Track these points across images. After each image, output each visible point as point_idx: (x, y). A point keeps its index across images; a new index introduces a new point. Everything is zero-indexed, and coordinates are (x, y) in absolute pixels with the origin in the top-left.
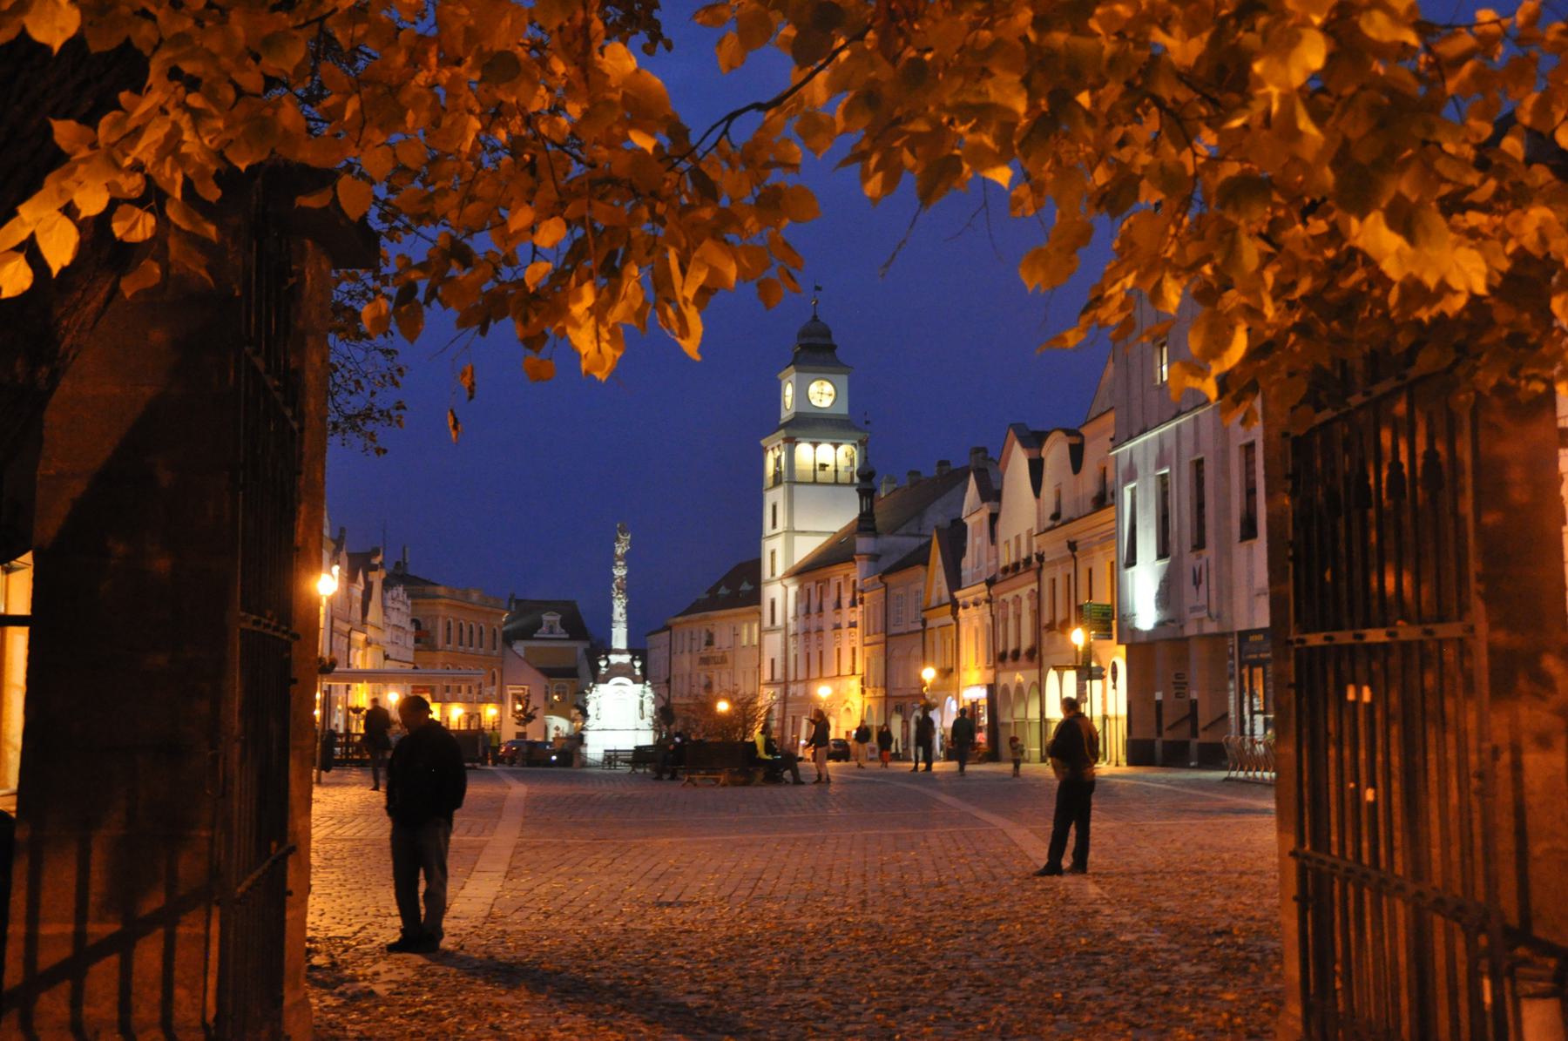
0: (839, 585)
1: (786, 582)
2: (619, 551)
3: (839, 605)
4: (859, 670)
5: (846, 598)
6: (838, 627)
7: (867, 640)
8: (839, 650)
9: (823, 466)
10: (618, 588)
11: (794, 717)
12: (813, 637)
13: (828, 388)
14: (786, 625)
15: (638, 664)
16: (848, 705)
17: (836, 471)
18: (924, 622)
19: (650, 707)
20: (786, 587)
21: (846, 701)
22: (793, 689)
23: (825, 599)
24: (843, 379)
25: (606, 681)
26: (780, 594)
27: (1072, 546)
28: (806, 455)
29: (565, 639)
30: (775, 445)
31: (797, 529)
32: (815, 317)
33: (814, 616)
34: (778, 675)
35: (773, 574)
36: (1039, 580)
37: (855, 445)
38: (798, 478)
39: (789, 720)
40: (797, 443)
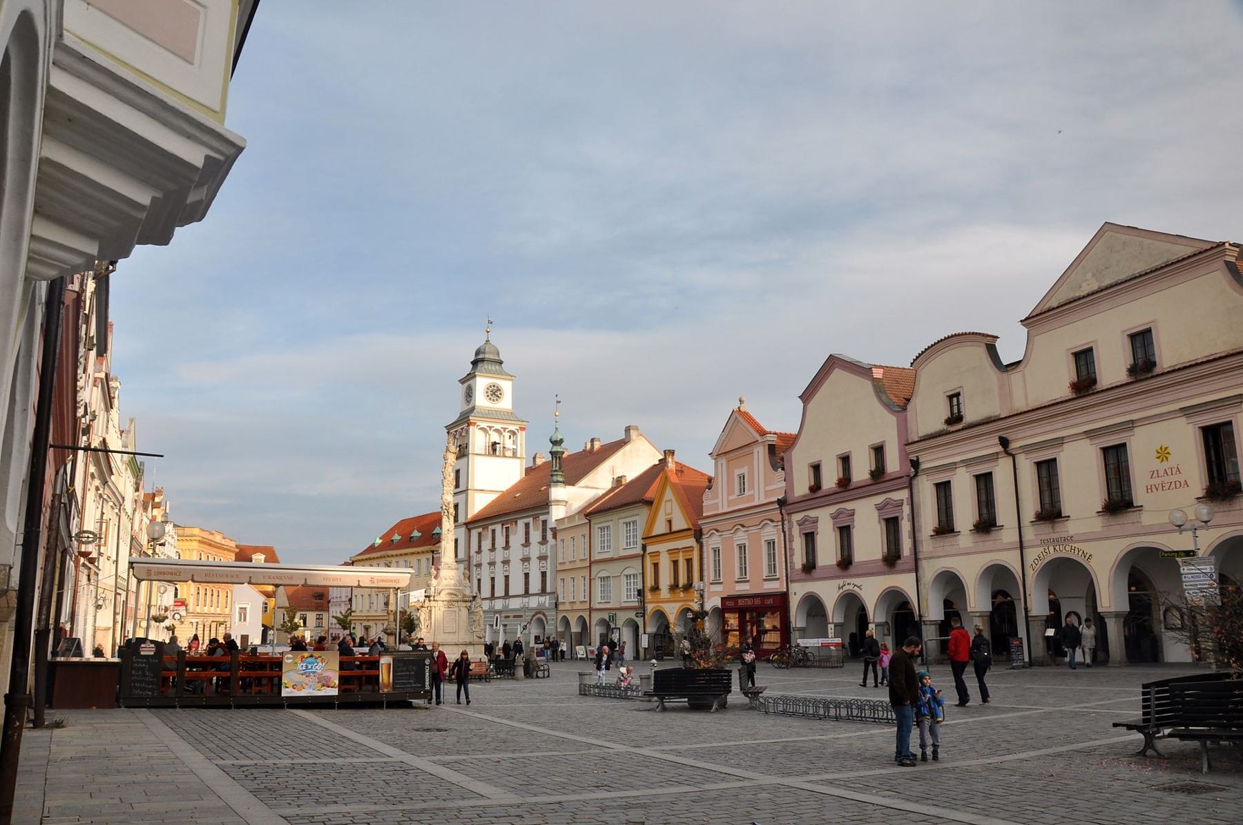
0: (527, 525)
1: (470, 526)
5: (536, 536)
12: (499, 565)
20: (469, 530)
23: (511, 538)
27: (1004, 442)
31: (476, 488)
36: (910, 487)
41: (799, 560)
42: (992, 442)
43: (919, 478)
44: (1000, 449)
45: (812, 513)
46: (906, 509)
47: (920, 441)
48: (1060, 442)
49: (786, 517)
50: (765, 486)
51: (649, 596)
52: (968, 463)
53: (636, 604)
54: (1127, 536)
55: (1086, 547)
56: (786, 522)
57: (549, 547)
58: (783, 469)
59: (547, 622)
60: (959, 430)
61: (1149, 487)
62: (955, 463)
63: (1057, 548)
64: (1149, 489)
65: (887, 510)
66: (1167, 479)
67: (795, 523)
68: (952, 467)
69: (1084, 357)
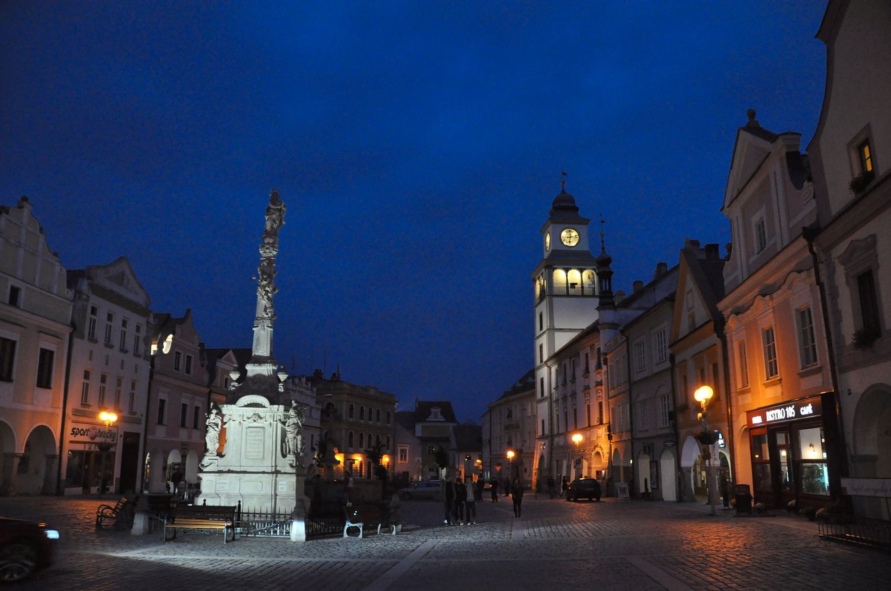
0: (587, 355)
1: (549, 363)
2: (268, 225)
3: (587, 371)
4: (604, 422)
5: (593, 363)
6: (587, 388)
7: (611, 394)
8: (589, 406)
9: (573, 285)
10: (263, 273)
11: (557, 461)
12: (569, 399)
13: (574, 233)
14: (551, 394)
15: (283, 377)
16: (598, 449)
17: (582, 287)
18: (672, 358)
19: (294, 441)
20: (550, 368)
21: (596, 446)
22: (556, 439)
24: (584, 228)
25: (232, 400)
26: (547, 374)
28: (560, 275)
29: (444, 421)
30: (540, 274)
31: (556, 328)
32: (563, 191)
33: (569, 384)
34: (547, 432)
35: (541, 361)
37: (595, 270)
38: (555, 292)
39: (555, 463)
40: (554, 269)
41: (849, 327)
45: (862, 234)
49: (822, 257)
50: (789, 219)
51: (680, 419)
53: (667, 431)
56: (822, 267)
57: (603, 375)
58: (810, 179)
59: (603, 456)
67: (836, 262)
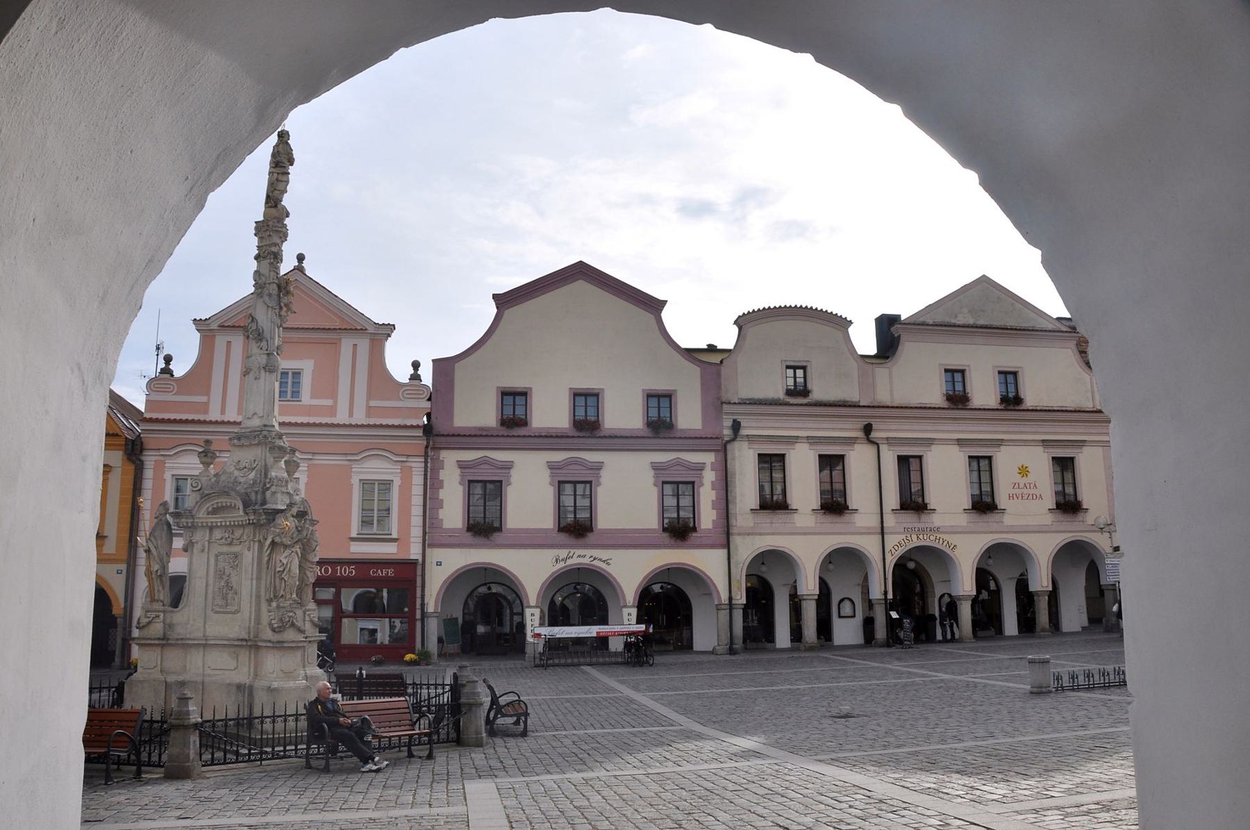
27: (868, 429)
42: (851, 426)
43: (736, 444)
44: (860, 434)
46: (709, 476)
47: (740, 403)
48: (929, 442)
52: (812, 441)
54: (991, 532)
55: (953, 539)
60: (801, 405)
61: (1011, 495)
62: (797, 437)
63: (921, 537)
64: (1011, 497)
65: (568, 471)
66: (1025, 491)
68: (792, 440)
69: (955, 374)
